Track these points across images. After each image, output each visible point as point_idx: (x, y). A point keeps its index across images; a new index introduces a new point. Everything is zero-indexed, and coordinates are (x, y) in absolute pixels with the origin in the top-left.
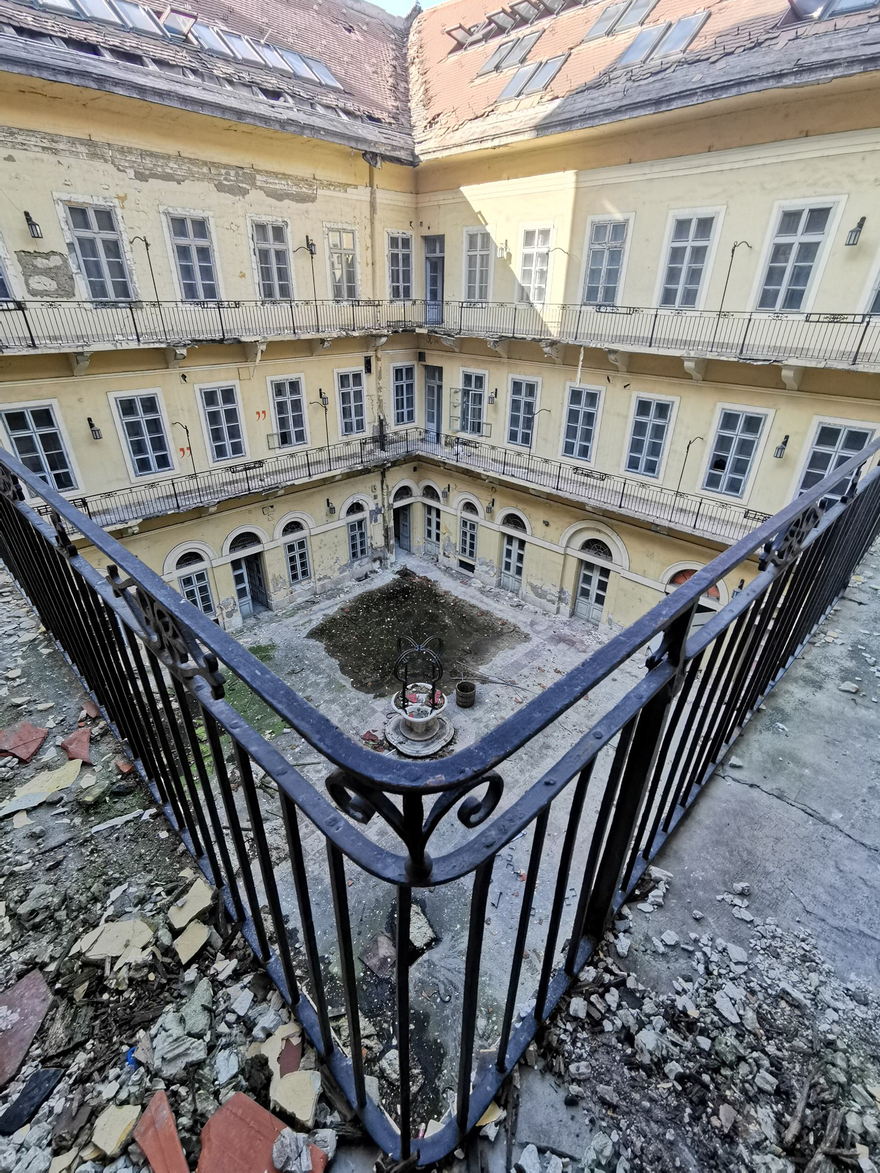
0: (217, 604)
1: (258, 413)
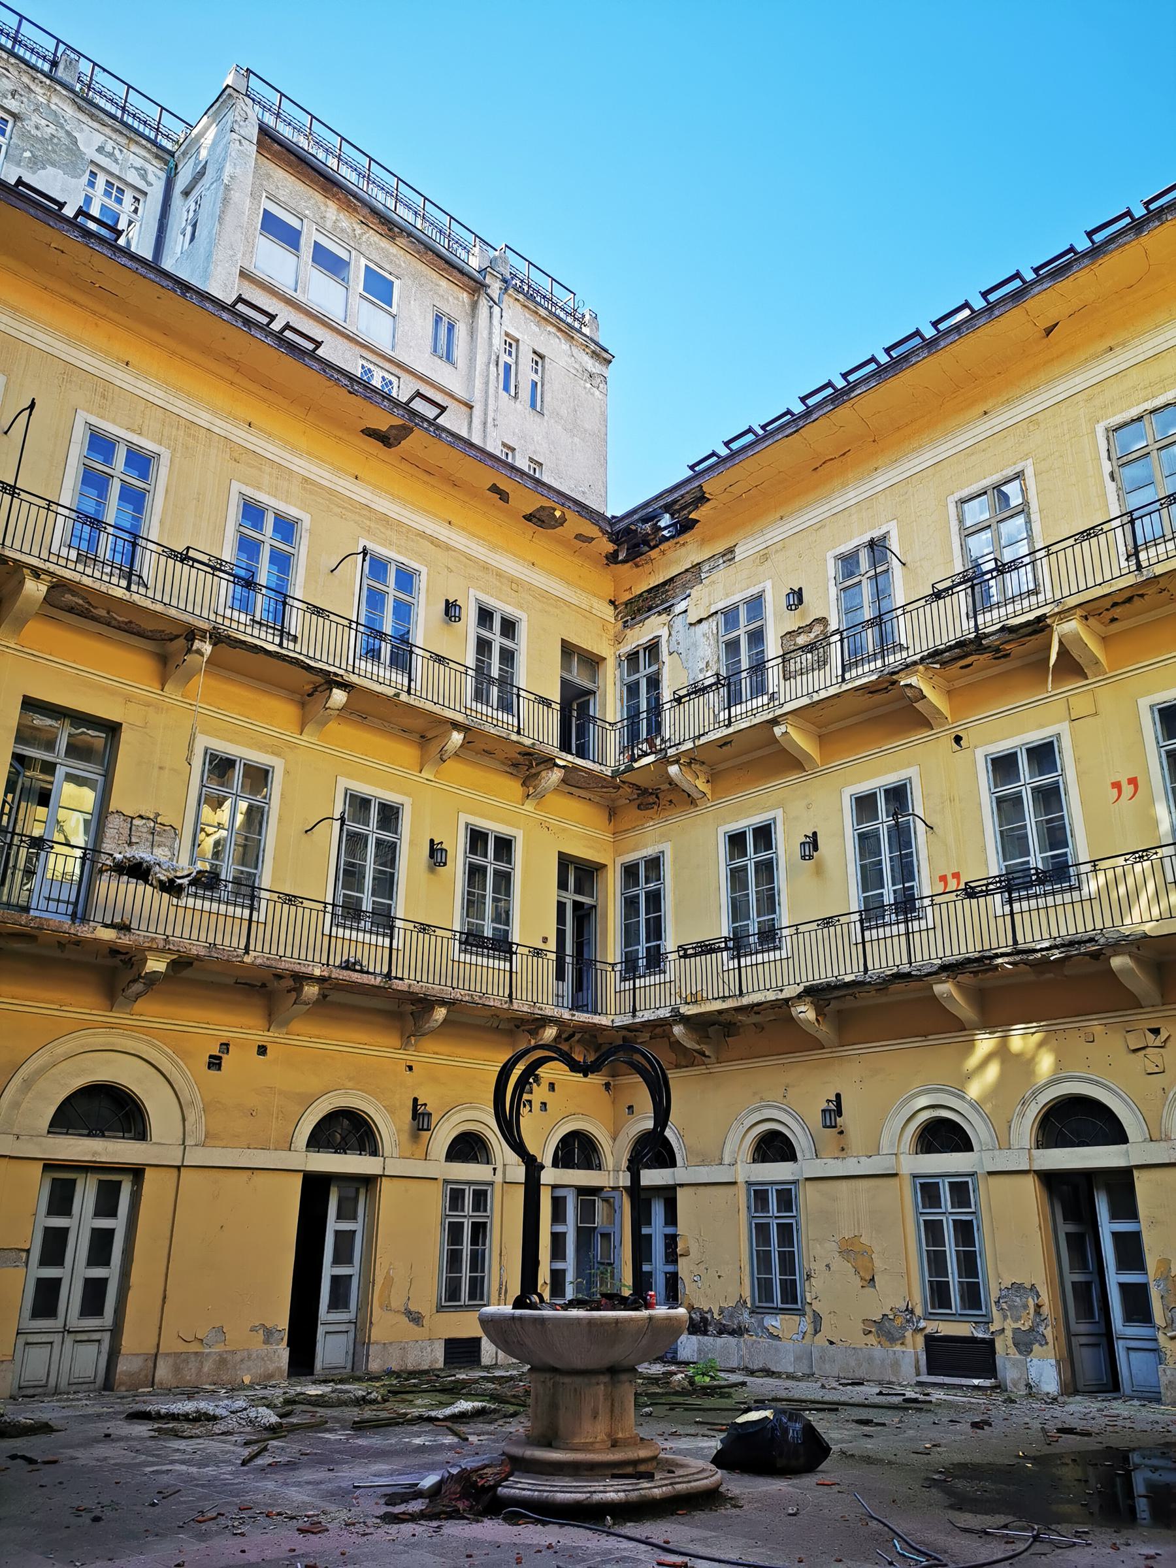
0: (994, 1294)
1: (1117, 785)
